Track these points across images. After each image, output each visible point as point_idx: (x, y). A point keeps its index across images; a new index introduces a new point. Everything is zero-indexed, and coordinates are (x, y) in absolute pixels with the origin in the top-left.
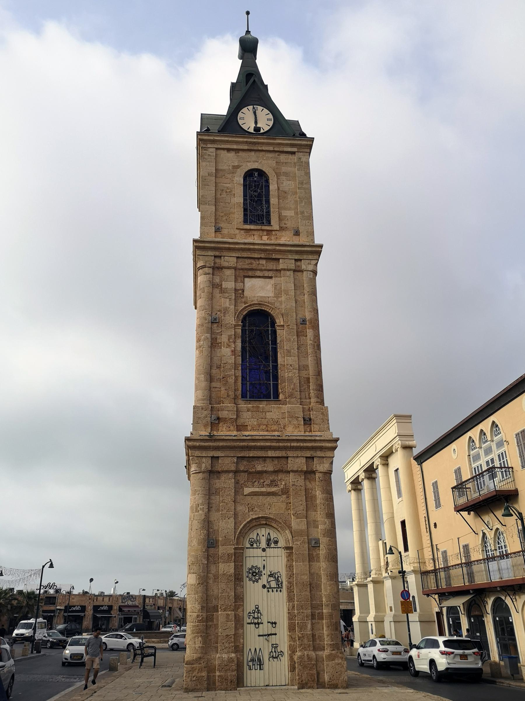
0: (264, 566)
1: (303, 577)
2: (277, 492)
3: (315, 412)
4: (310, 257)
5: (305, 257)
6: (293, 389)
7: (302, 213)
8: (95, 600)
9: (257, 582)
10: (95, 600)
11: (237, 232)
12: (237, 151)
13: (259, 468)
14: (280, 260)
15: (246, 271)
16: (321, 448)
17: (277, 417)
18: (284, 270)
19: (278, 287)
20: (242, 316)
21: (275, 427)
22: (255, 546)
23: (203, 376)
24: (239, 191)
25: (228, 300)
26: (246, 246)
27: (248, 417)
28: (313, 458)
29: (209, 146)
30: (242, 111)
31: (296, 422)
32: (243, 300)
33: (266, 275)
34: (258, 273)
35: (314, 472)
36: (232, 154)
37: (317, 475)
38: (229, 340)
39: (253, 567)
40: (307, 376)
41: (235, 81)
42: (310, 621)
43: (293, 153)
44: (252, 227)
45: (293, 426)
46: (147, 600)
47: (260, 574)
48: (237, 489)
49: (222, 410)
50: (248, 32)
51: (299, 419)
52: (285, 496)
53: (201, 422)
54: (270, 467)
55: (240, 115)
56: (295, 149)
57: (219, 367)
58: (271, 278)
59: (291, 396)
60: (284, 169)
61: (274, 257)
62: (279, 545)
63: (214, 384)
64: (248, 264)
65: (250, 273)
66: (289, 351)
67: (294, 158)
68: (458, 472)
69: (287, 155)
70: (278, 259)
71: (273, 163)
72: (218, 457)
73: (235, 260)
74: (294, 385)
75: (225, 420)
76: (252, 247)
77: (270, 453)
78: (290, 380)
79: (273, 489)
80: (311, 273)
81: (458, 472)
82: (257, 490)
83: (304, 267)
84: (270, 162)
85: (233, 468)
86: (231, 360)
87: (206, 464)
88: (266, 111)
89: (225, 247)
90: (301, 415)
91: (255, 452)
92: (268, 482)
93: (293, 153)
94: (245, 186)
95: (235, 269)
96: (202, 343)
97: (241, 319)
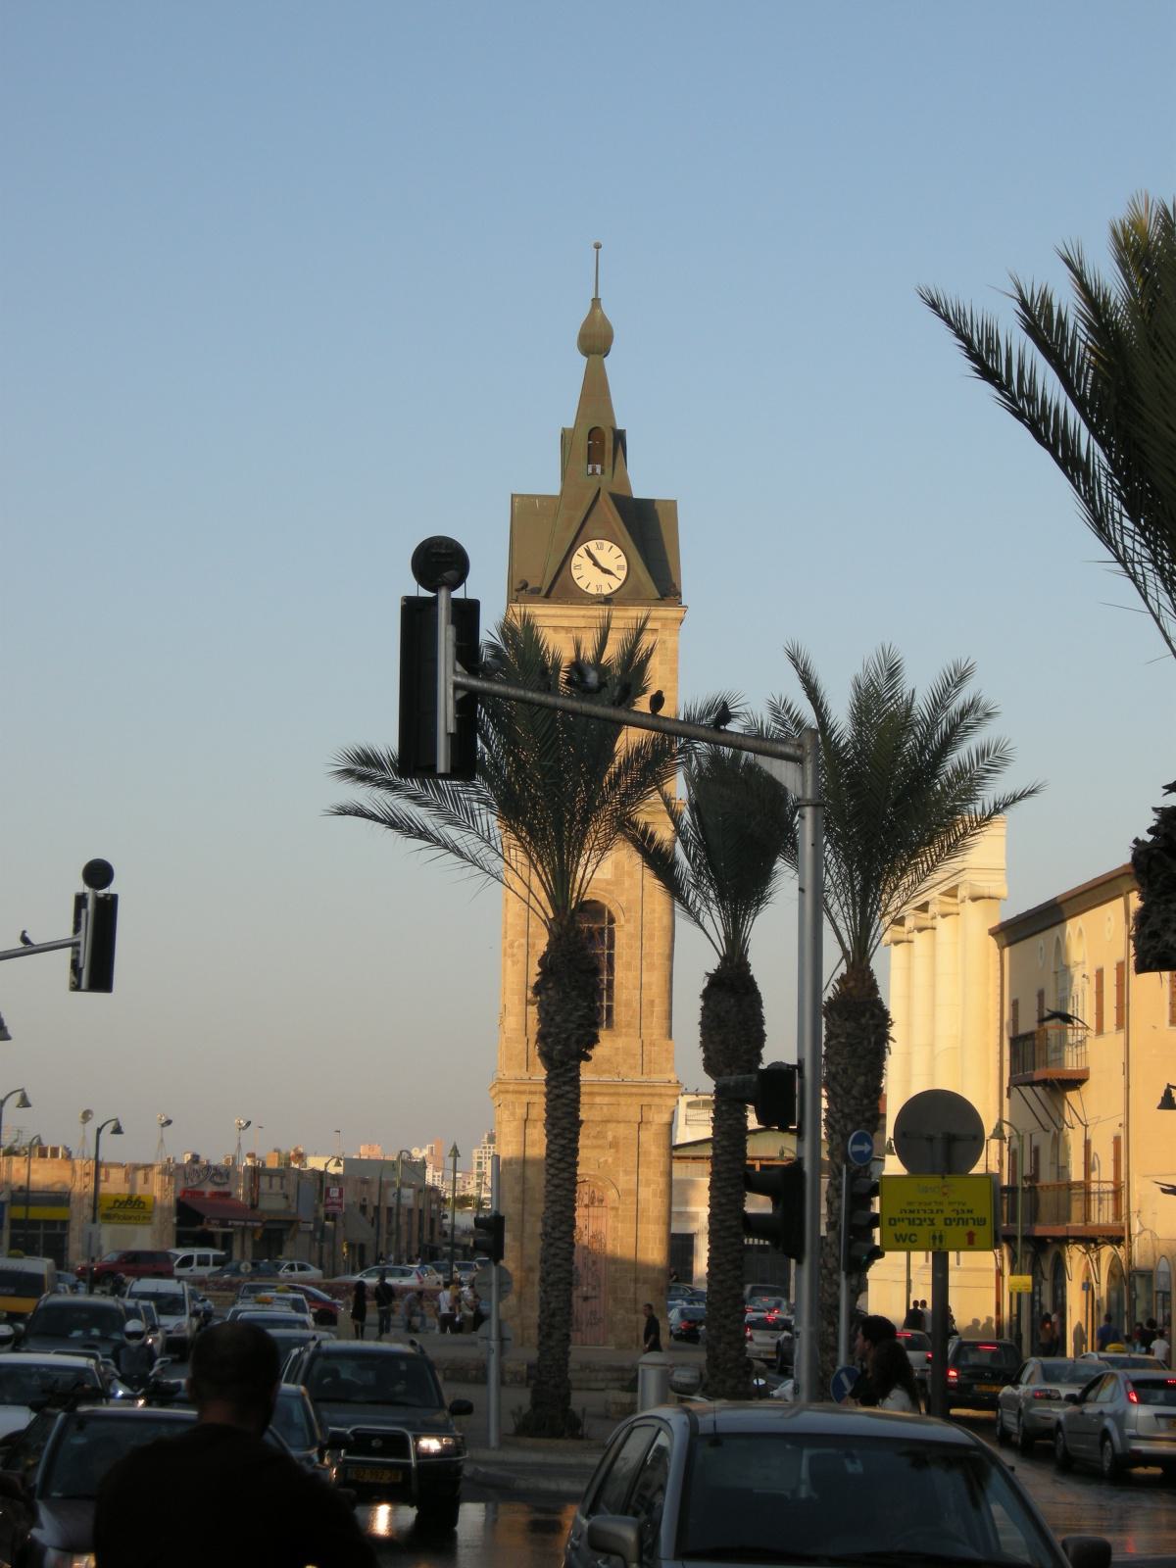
6: (632, 1017)
16: (660, 1095)
23: (516, 997)
28: (649, 1106)
41: (570, 425)
46: (264, 1182)
50: (596, 302)
52: (612, 1150)
59: (629, 1025)
68: (1041, 995)
78: (628, 1004)
79: (600, 1142)
81: (1041, 995)
87: (521, 1112)
88: (617, 551)
96: (515, 950)
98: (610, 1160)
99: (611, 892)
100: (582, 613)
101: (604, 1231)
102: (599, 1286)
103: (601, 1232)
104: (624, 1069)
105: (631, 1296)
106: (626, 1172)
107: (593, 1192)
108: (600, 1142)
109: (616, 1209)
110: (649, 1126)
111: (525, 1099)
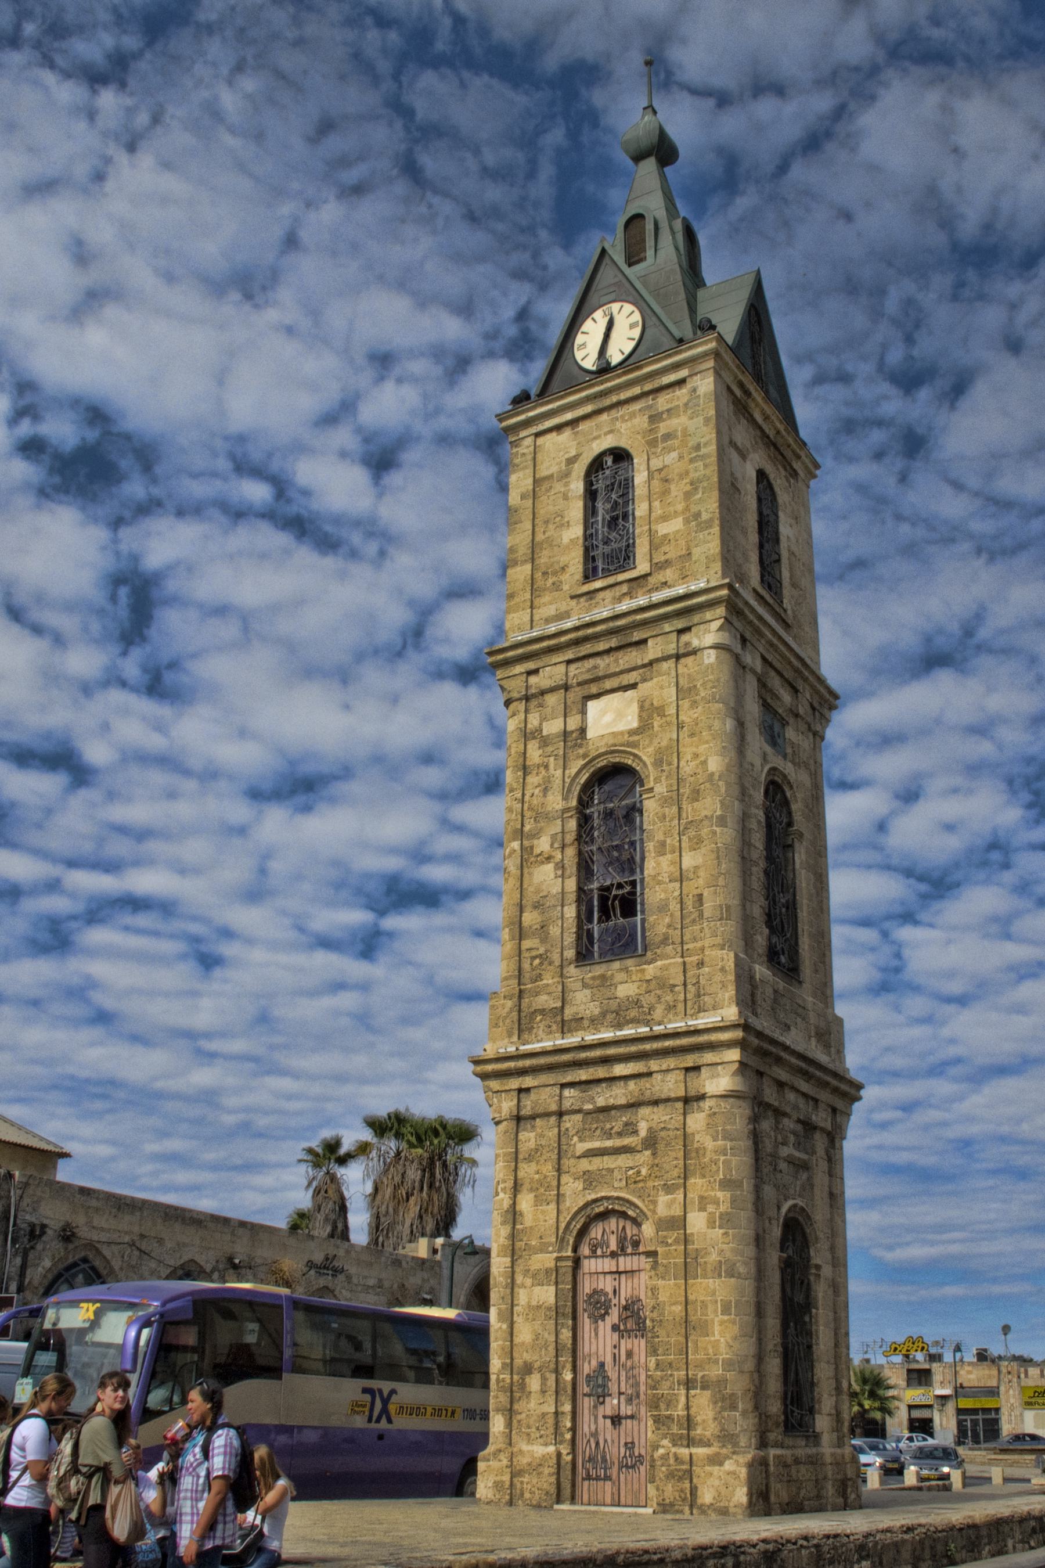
0: (615, 1291)
1: (673, 1308)
2: (633, 1145)
3: (707, 969)
4: (708, 615)
5: (696, 618)
6: (669, 926)
7: (698, 515)
8: (1022, 1376)
9: (603, 1320)
10: (1022, 1376)
11: (574, 602)
12: (573, 423)
13: (601, 1102)
14: (650, 642)
15: (586, 686)
17: (637, 991)
18: (658, 660)
19: (647, 705)
20: (578, 788)
21: (633, 1013)
22: (599, 1252)
24: (576, 510)
25: (552, 759)
26: (580, 633)
27: (584, 1000)
28: (697, 1068)
29: (522, 434)
30: (584, 328)
31: (669, 998)
32: (581, 751)
33: (625, 683)
34: (608, 684)
35: (702, 1097)
36: (567, 433)
37: (707, 1104)
38: (552, 846)
39: (595, 1292)
40: (699, 891)
42: (683, 1392)
43: (681, 382)
44: (598, 584)
45: (663, 1007)
47: (607, 1307)
48: (564, 1147)
49: (537, 994)
51: (677, 989)
52: (648, 1153)
53: (501, 1024)
54: (618, 1095)
55: (580, 339)
56: (683, 373)
57: (537, 906)
58: (634, 686)
59: (665, 940)
60: (663, 428)
61: (637, 639)
62: (641, 1249)
63: (526, 944)
64: (589, 670)
65: (594, 689)
66: (663, 844)
67: (682, 393)
69: (670, 390)
70: (644, 641)
71: (641, 422)
72: (528, 1090)
73: (562, 668)
74: (672, 915)
75: (542, 1011)
76: (590, 631)
77: (619, 1070)
78: (663, 908)
79: (627, 1141)
80: (712, 652)
82: (597, 1144)
83: (695, 643)
84: (636, 421)
85: (554, 1107)
86: (556, 889)
87: (507, 1105)
88: (628, 308)
89: (541, 649)
90: (679, 980)
91: (591, 1070)
92: (618, 1126)
93: (681, 382)
94: (591, 495)
95: (566, 687)
97: (576, 793)
98: (644, 1172)
99: (635, 745)
100: (584, 394)
101: (642, 1297)
102: (638, 1396)
103: (640, 1300)
104: (658, 1013)
105: (680, 1411)
106: (669, 1189)
107: (624, 1228)
108: (627, 1141)
109: (653, 1254)
110: (701, 1104)
111: (514, 1083)
